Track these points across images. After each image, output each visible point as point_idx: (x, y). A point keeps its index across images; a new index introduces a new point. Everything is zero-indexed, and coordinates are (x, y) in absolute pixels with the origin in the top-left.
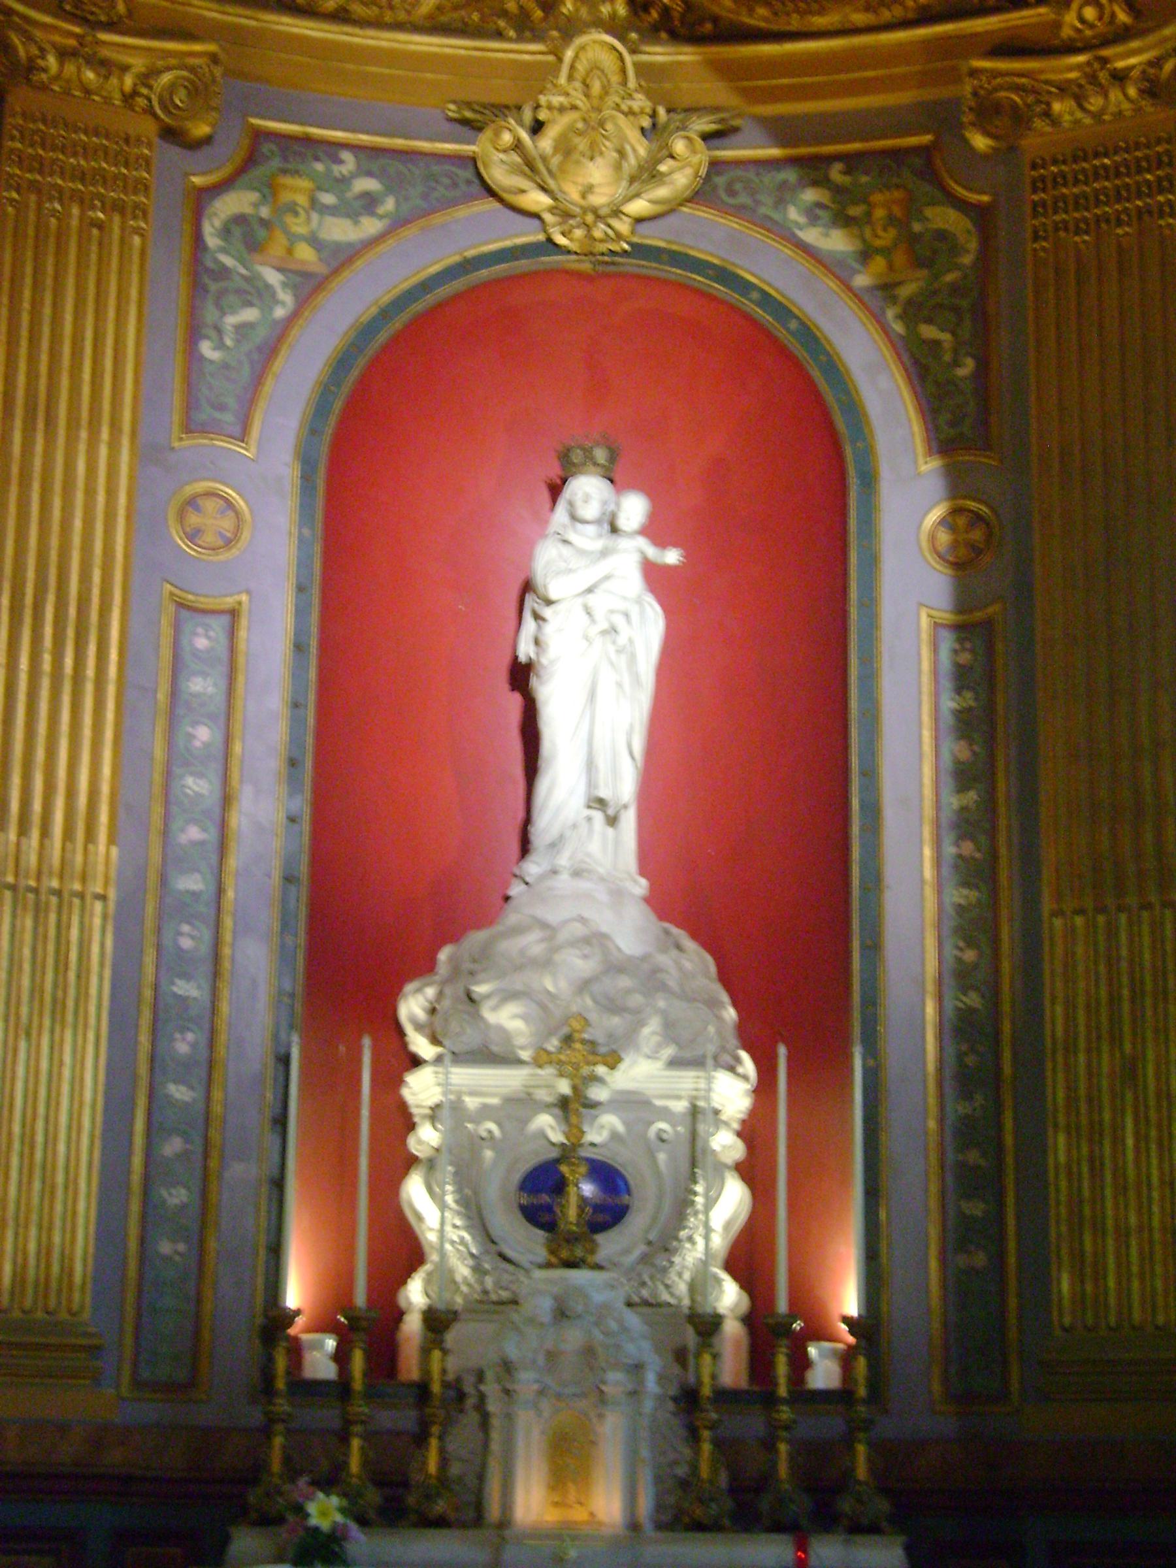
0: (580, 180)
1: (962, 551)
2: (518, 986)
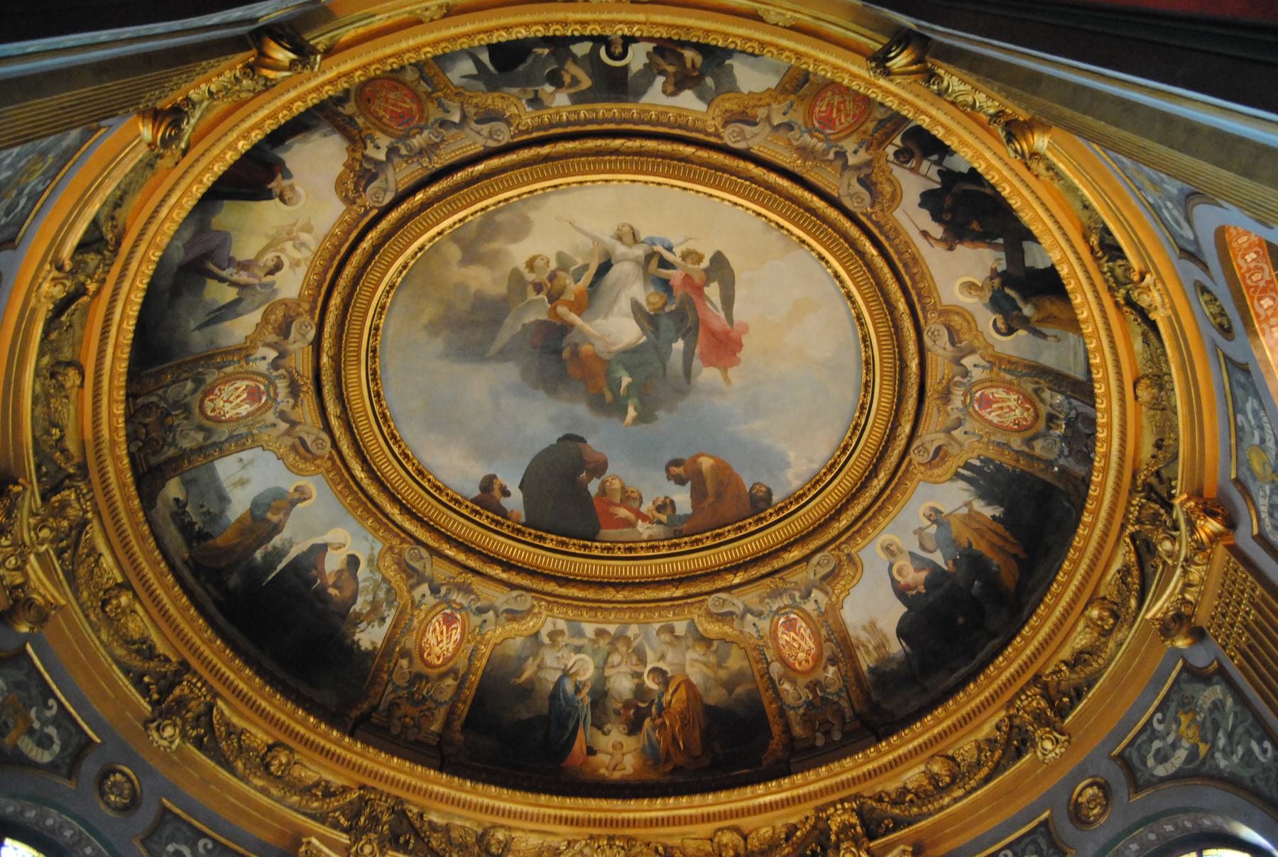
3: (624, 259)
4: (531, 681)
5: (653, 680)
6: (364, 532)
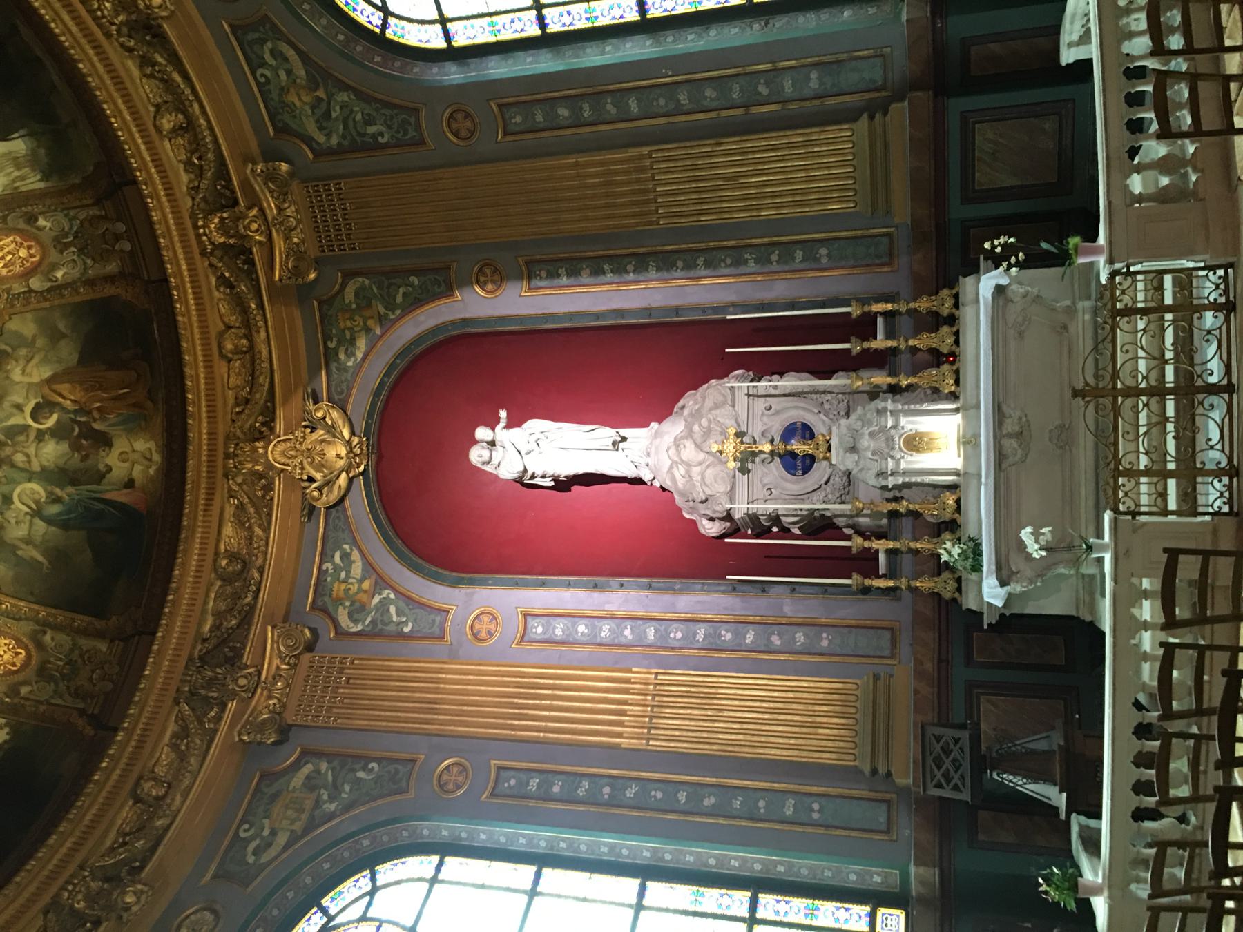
1: (496, 277)
2: (699, 478)
4: (45, 553)
5: (47, 418)
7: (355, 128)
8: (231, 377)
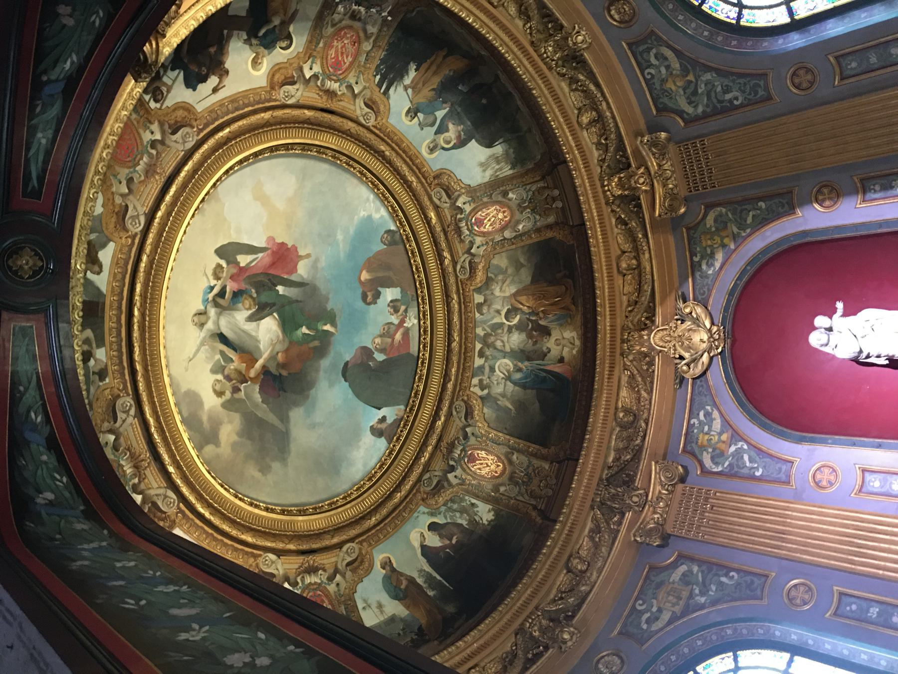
0: (699, 343)
1: (833, 195)
3: (217, 323)
5: (514, 318)
6: (413, 519)
7: (716, 97)
8: (625, 286)
